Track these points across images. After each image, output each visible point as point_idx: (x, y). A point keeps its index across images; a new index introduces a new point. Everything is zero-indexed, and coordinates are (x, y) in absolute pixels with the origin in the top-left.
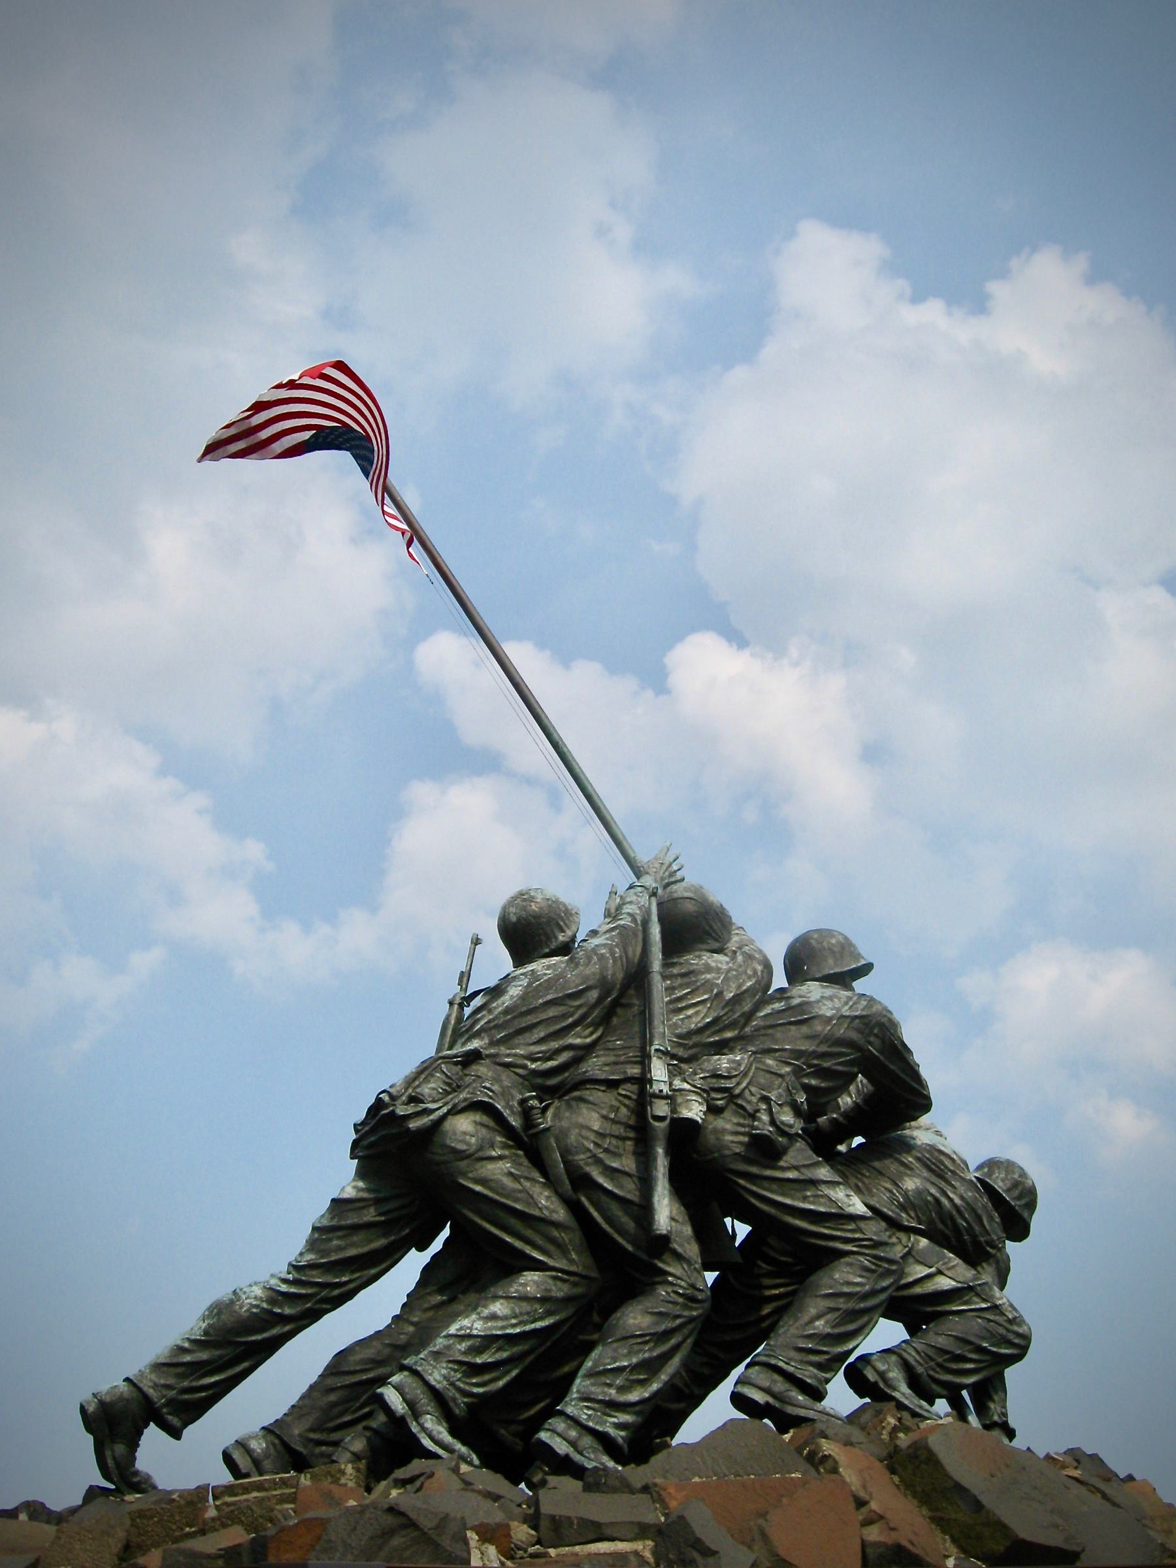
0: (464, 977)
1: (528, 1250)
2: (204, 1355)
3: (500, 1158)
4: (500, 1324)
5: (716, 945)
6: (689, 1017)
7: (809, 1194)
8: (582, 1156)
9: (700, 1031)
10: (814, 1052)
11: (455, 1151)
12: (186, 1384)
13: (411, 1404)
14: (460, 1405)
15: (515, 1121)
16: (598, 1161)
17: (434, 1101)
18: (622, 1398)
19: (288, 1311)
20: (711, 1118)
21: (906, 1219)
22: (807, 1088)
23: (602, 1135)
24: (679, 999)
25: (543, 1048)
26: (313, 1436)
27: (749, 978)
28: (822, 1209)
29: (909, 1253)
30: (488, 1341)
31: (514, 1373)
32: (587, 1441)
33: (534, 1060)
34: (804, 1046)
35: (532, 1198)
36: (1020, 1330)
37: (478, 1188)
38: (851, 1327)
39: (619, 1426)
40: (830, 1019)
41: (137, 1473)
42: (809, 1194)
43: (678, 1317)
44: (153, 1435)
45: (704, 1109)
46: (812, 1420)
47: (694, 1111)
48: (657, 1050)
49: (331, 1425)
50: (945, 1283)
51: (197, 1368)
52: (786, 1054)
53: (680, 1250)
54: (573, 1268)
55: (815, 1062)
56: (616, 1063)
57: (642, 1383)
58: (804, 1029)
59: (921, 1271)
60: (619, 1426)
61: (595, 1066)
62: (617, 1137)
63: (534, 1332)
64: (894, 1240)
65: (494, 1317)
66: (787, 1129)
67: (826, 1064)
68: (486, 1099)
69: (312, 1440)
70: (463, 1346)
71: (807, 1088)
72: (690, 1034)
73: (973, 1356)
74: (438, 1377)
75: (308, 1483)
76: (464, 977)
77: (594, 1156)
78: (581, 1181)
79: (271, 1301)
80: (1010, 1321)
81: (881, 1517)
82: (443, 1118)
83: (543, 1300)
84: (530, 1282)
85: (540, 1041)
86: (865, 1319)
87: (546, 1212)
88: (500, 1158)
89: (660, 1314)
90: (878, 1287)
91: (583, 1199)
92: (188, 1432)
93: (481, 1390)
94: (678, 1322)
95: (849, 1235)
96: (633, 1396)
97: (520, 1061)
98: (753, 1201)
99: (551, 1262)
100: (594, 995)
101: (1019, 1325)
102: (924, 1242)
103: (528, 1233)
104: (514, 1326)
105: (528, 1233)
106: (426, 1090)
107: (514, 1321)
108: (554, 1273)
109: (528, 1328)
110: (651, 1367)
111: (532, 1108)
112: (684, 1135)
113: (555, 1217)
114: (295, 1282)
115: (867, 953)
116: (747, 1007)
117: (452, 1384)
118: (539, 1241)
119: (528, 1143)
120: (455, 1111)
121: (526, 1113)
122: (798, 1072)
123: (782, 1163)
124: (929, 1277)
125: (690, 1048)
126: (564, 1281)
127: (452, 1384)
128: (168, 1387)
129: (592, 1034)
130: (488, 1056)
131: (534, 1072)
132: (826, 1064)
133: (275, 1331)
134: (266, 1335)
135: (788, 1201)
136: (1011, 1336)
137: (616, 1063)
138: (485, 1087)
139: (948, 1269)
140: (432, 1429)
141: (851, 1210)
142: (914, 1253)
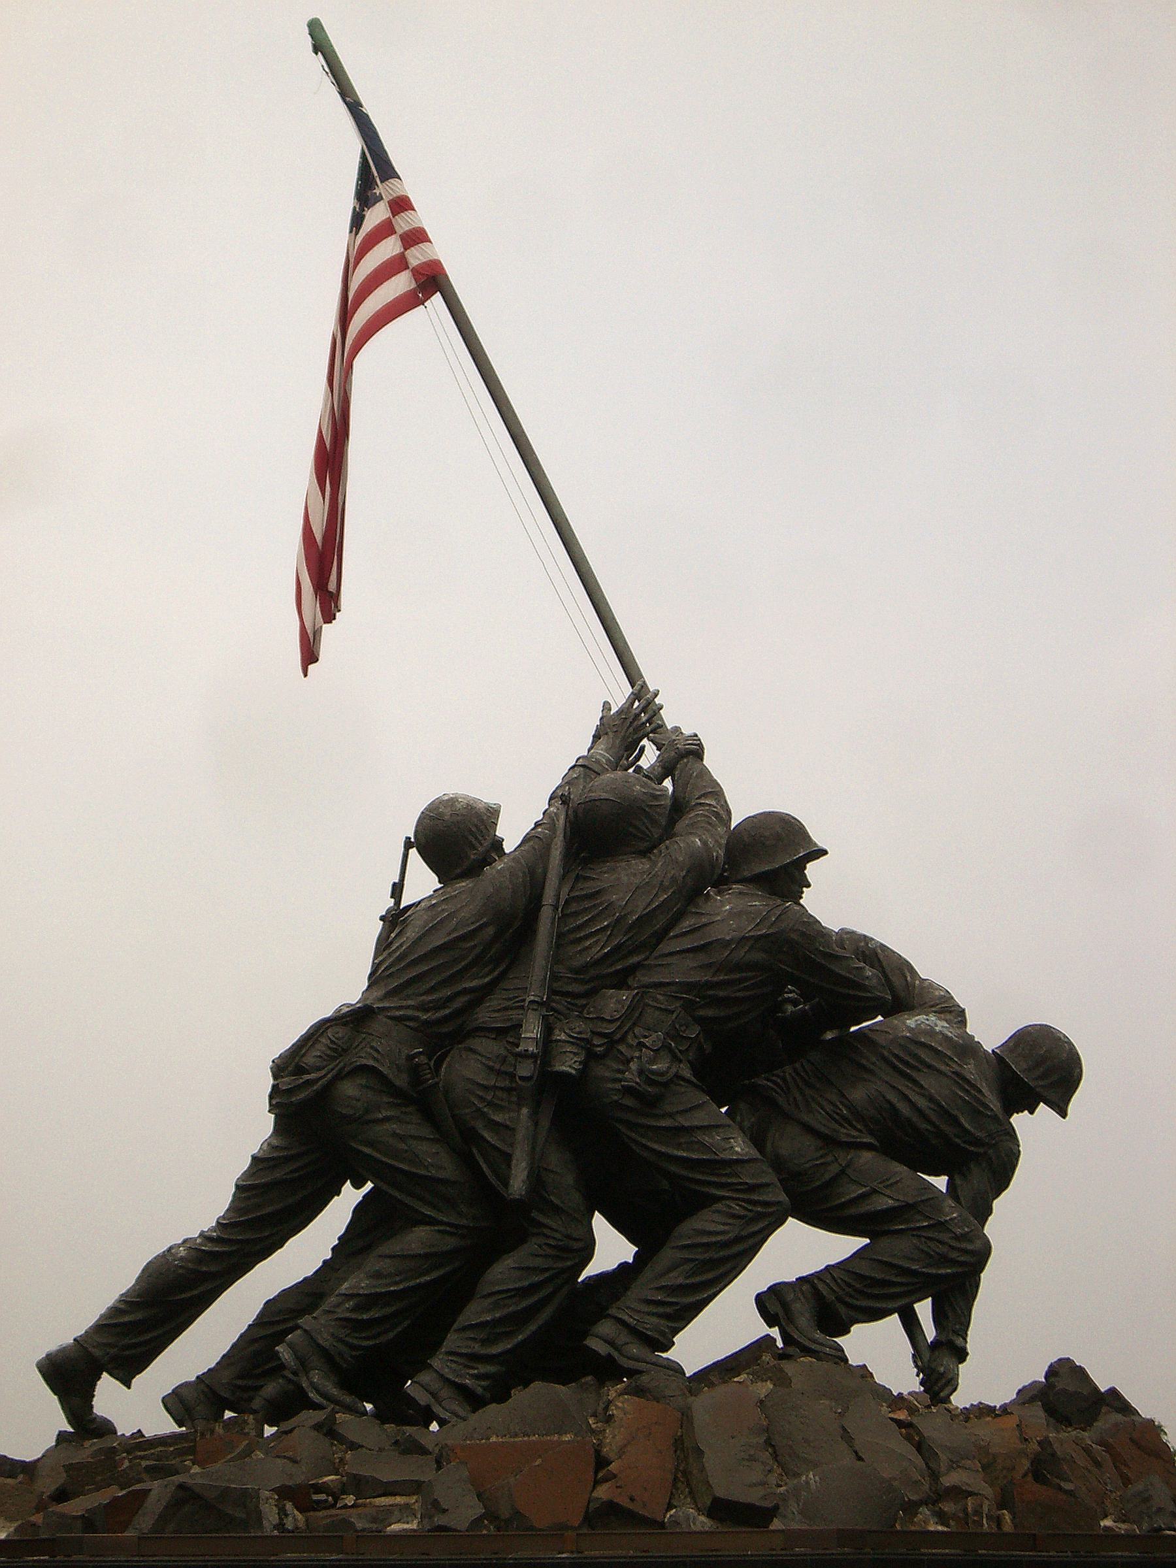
0: (397, 890)
1: (417, 1205)
2: (139, 1316)
3: (387, 1119)
4: (384, 1281)
5: (644, 845)
6: (587, 948)
7: (682, 1140)
8: (467, 1111)
9: (597, 963)
10: (707, 981)
12: (127, 1341)
13: (302, 1361)
15: (401, 1081)
16: (484, 1115)
17: (319, 1069)
19: (213, 1268)
21: (845, 1133)
22: (700, 1021)
23: (486, 1088)
24: (580, 928)
25: (434, 997)
26: (239, 1382)
27: (665, 891)
29: (843, 1172)
30: (372, 1300)
31: (406, 1323)
32: (445, 1393)
33: (427, 1010)
34: (695, 978)
35: (417, 1156)
36: (970, 1247)
38: (710, 1276)
40: (729, 942)
41: (95, 1419)
42: (682, 1140)
43: (547, 1270)
46: (640, 1372)
47: (568, 1064)
48: (532, 1002)
49: (259, 1371)
52: (673, 988)
54: (464, 1222)
55: (711, 992)
56: (506, 1009)
57: (508, 1335)
58: (702, 958)
60: (478, 1377)
61: (485, 1015)
62: (502, 1089)
63: (419, 1286)
64: (830, 1158)
65: (378, 1275)
66: (659, 1079)
68: (371, 1063)
69: (240, 1387)
70: (350, 1304)
71: (700, 1021)
72: (585, 968)
73: (898, 1279)
74: (325, 1335)
75: (221, 1431)
76: (397, 890)
77: (479, 1110)
78: (470, 1136)
79: (200, 1261)
80: (957, 1238)
81: (615, 1476)
83: (426, 1256)
84: (417, 1239)
85: (432, 990)
86: (729, 1266)
87: (434, 1172)
88: (387, 1119)
89: (528, 1268)
90: (744, 1233)
91: (475, 1151)
92: (137, 1381)
93: (371, 1343)
94: (547, 1275)
95: (724, 1180)
96: (495, 1350)
97: (410, 1012)
99: (441, 1217)
100: (491, 930)
101: (971, 1241)
102: (867, 1156)
104: (396, 1283)
106: (310, 1060)
107: (398, 1279)
108: (442, 1228)
109: (412, 1283)
110: (519, 1319)
111: (418, 1065)
113: (441, 1175)
115: (819, 837)
116: (660, 922)
117: (341, 1340)
119: (420, 1097)
120: (339, 1077)
121: (415, 1071)
122: (689, 1006)
124: (863, 1196)
125: (587, 982)
126: (451, 1234)
127: (341, 1340)
128: (109, 1345)
129: (490, 972)
130: (384, 1009)
131: (426, 1022)
132: (721, 994)
133: (201, 1289)
134: (195, 1292)
135: (663, 1149)
136: (954, 1255)
137: (506, 1009)
138: (372, 1047)
139: (887, 1187)
142: (849, 1171)
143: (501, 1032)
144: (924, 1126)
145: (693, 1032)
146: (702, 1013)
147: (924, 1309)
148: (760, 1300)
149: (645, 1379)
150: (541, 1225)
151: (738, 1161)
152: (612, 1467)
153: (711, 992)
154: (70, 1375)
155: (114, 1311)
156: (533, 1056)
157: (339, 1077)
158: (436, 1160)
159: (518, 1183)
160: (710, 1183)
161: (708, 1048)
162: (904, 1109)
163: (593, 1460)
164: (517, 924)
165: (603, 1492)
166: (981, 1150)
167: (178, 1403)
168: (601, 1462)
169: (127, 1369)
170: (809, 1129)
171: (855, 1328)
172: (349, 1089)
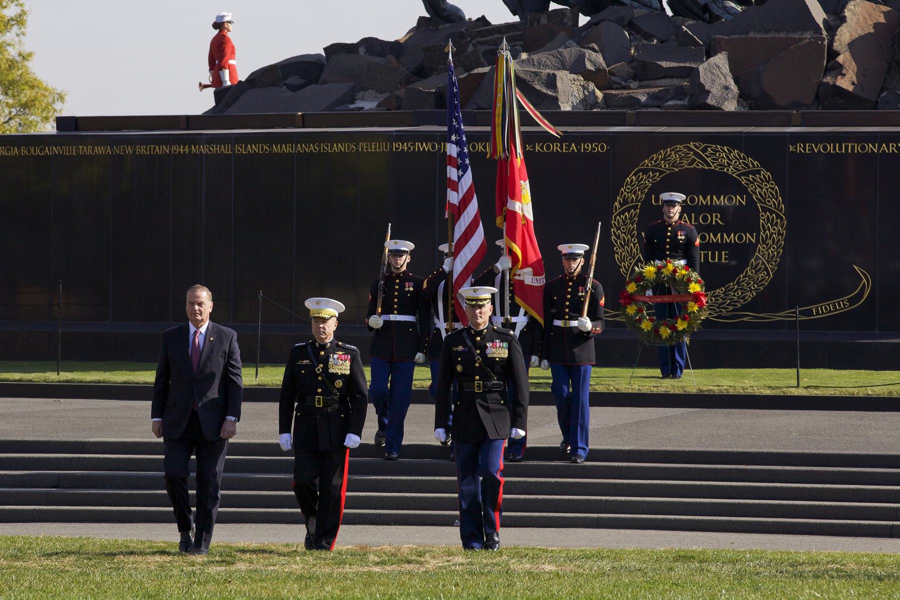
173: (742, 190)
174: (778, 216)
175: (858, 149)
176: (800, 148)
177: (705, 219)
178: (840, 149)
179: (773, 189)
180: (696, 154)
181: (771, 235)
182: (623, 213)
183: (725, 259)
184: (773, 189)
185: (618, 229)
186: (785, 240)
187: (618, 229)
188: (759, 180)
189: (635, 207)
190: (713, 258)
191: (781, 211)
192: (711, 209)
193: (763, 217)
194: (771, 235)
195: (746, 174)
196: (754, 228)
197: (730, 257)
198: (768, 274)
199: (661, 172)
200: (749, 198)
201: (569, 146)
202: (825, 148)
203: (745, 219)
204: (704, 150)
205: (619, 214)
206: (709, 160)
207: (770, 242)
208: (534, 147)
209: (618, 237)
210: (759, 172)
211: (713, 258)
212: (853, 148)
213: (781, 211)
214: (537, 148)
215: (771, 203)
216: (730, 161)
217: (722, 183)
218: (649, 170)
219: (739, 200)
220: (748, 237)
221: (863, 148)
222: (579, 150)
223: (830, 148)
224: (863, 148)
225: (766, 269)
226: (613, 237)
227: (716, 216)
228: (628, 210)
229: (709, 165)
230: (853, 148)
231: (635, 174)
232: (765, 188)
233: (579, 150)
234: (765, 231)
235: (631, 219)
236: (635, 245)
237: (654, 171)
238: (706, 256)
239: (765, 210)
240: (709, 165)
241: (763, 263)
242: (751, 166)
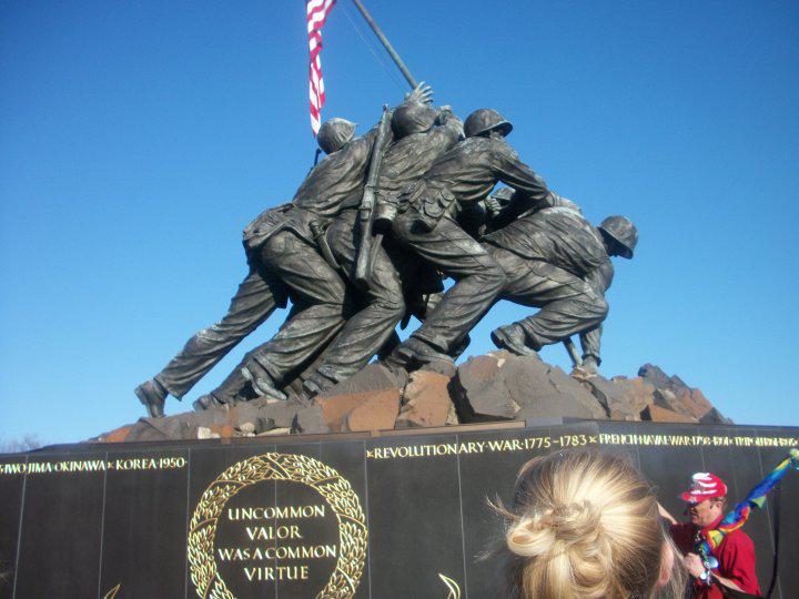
11: (277, 254)
14: (277, 373)
18: (346, 361)
20: (400, 216)
21: (530, 254)
28: (454, 254)
31: (308, 355)
37: (287, 269)
39: (347, 374)
44: (170, 400)
45: (395, 211)
47: (389, 214)
50: (552, 284)
51: (182, 369)
53: (383, 284)
59: (538, 279)
67: (465, 178)
71: (456, 193)
78: (340, 259)
82: (269, 239)
96: (352, 359)
98: (426, 256)
102: (543, 264)
103: (314, 287)
105: (314, 287)
112: (381, 226)
114: (222, 325)
118: (319, 290)
120: (276, 234)
123: (433, 233)
131: (320, 209)
136: (592, 309)
140: (264, 385)
141: (472, 252)
143: (356, 207)
144: (569, 251)
145: (451, 197)
146: (454, 189)
147: (576, 339)
148: (494, 336)
149: (431, 365)
150: (376, 297)
151: (479, 255)
152: (410, 403)
153: (460, 178)
154: (152, 397)
155: (173, 362)
156: (369, 210)
157: (276, 234)
158: (321, 270)
159: (361, 272)
160: (465, 268)
161: (460, 209)
162: (560, 243)
163: (398, 401)
164: (364, 162)
165: (403, 417)
166: (597, 265)
167: (199, 403)
168: (403, 401)
169: (183, 389)
170: (514, 253)
171: (544, 348)
172: (280, 240)
173: (320, 501)
174: (359, 527)
175: (436, 450)
176: (377, 454)
177: (283, 532)
178: (419, 452)
179: (351, 498)
180: (273, 465)
181: (352, 547)
182: (199, 529)
183: (305, 575)
184: (351, 498)
185: (195, 547)
186: (366, 551)
187: (195, 547)
188: (337, 489)
189: (212, 523)
190: (292, 574)
191: (361, 520)
192: (289, 522)
193: (343, 530)
194: (352, 547)
195: (324, 483)
196: (333, 539)
197: (310, 573)
198: (351, 590)
199: (238, 485)
200: (328, 508)
201: (148, 463)
202: (403, 452)
203: (321, 532)
204: (281, 461)
205: (196, 531)
206: (286, 470)
207: (352, 554)
208: (115, 465)
209: (195, 556)
210: (336, 480)
211: (292, 574)
212: (431, 450)
213: (361, 520)
214: (118, 466)
215: (352, 513)
216: (307, 468)
217: (300, 493)
218: (227, 483)
219: (319, 511)
220: (329, 551)
221: (442, 450)
222: (158, 466)
223: (408, 451)
224: (442, 450)
225: (348, 584)
226: (190, 556)
227: (295, 529)
228: (205, 526)
229: (285, 475)
230: (431, 450)
231: (213, 488)
232: (343, 498)
233: (158, 466)
234: (345, 542)
235: (208, 536)
236: (211, 563)
237: (231, 484)
238: (285, 573)
239: (344, 520)
240: (285, 475)
241: (345, 578)
242: (328, 474)
